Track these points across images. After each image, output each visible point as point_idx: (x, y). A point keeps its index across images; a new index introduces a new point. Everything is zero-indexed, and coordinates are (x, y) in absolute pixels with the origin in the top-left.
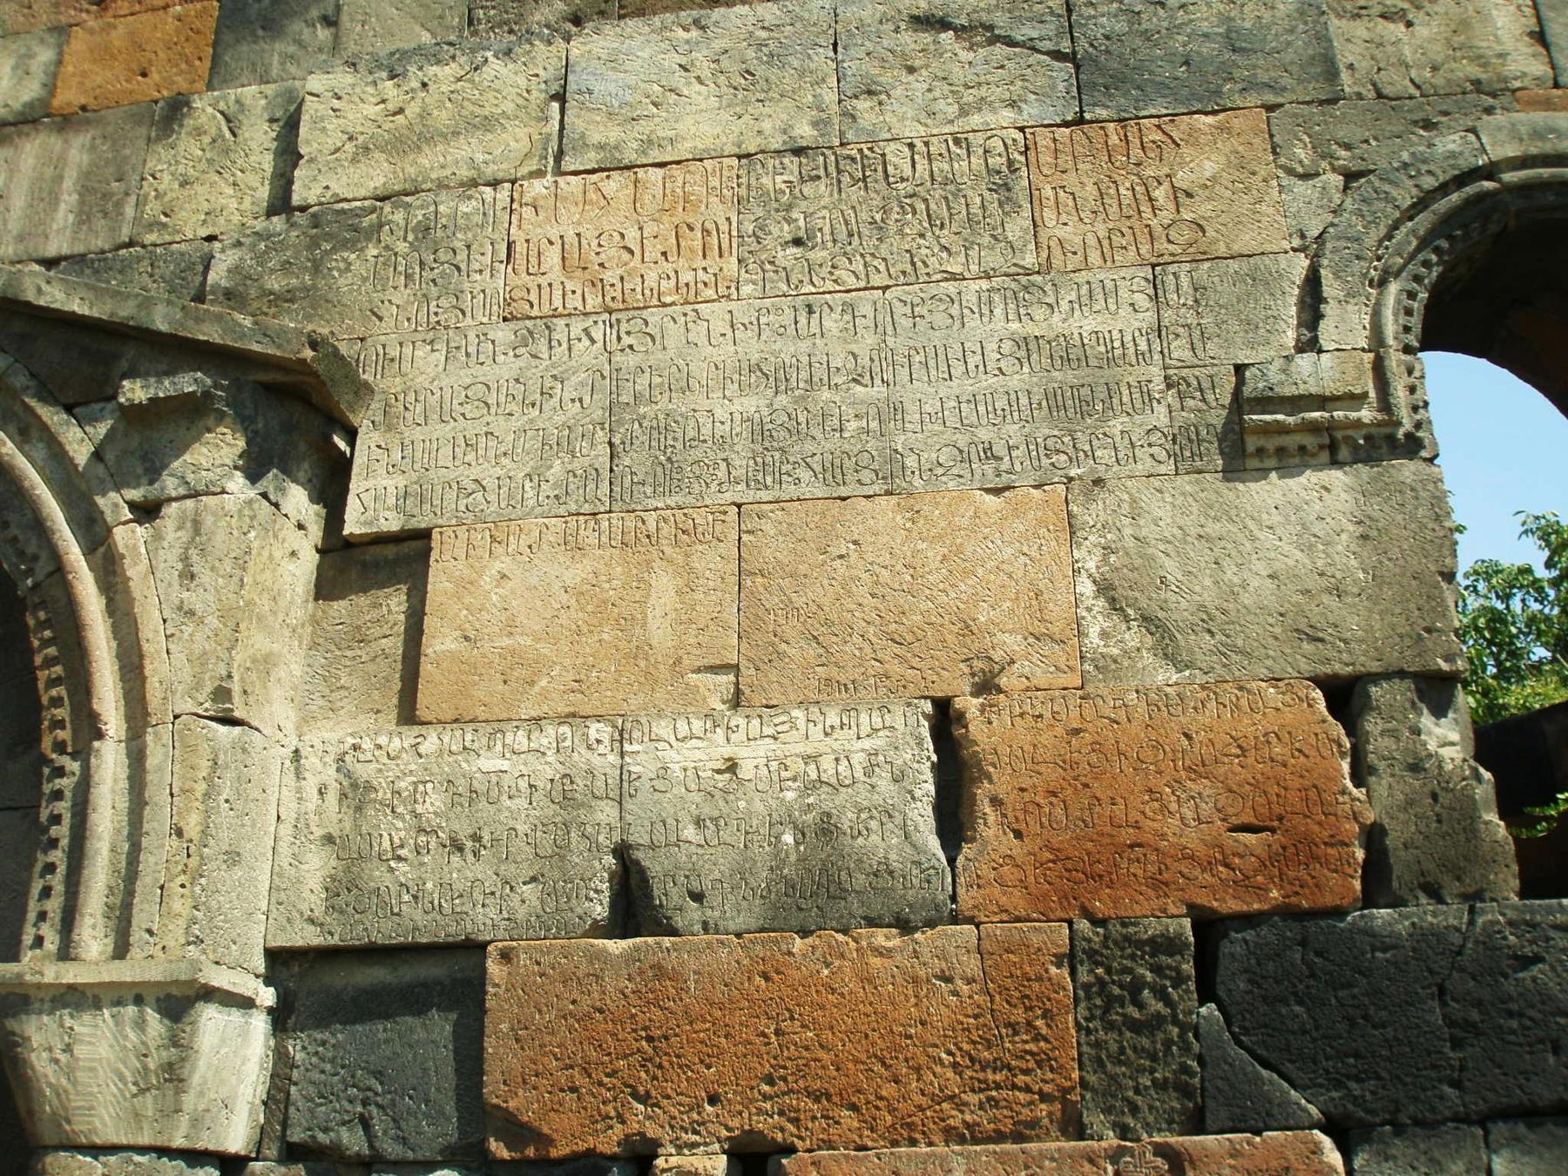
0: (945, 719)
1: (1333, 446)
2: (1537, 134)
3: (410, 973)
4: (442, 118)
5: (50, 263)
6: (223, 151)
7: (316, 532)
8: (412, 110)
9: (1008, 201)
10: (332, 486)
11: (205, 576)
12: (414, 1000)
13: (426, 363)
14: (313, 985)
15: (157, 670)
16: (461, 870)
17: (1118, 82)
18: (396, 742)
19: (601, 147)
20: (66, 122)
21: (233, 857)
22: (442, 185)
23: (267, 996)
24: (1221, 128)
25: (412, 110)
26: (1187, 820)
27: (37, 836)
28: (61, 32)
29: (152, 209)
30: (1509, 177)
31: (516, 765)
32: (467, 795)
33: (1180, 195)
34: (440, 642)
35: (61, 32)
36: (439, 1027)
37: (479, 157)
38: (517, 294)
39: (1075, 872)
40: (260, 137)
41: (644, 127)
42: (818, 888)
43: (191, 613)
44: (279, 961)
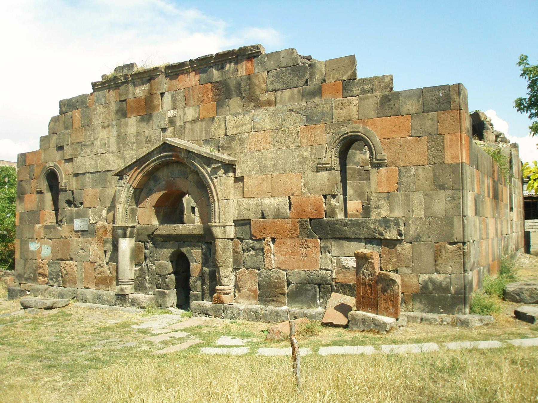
0: (289, 198)
1: (326, 169)
2: (353, 128)
3: (245, 222)
4: (241, 123)
5: (203, 140)
6: (219, 125)
7: (233, 176)
9: (298, 137)
10: (234, 171)
12: (246, 224)
13: (241, 156)
14: (238, 223)
16: (248, 213)
17: (310, 119)
20: (202, 120)
21: (228, 212)
23: (233, 224)
24: (320, 126)
26: (309, 209)
27: (211, 210)
28: (199, 105)
29: (213, 133)
30: (349, 134)
31: (253, 202)
32: (249, 205)
33: (315, 136)
34: (245, 189)
35: (199, 105)
36: (248, 227)
39: (299, 214)
40: (223, 123)
41: (262, 125)
42: (278, 215)
44: (234, 221)
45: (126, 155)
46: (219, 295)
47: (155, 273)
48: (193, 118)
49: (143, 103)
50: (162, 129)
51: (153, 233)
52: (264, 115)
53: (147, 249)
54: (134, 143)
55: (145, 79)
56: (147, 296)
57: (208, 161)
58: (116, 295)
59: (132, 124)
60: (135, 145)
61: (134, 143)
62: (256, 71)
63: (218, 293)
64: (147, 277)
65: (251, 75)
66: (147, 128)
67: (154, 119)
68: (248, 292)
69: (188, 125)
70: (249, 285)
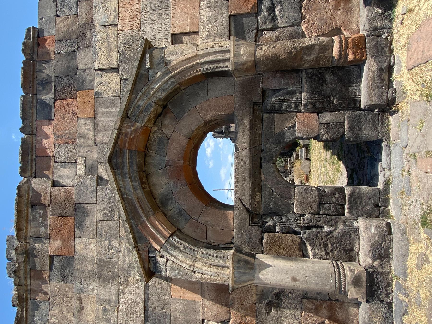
8: (103, 50)
11: (177, 51)
15: (190, 55)
16: (219, 20)
18: (202, 32)
19: (114, 18)
20: (96, 113)
22: (117, 43)
25: (103, 50)
32: (209, 21)
34: (188, 29)
37: (113, 37)
38: (137, 27)
43: (182, 52)
45: (125, 261)
46: (350, 45)
47: (316, 216)
48: (92, 129)
49: (60, 221)
50: (98, 185)
51: (247, 209)
52: (101, 10)
53: (275, 226)
54: (110, 244)
55: (29, 215)
56: (361, 229)
57: (141, 78)
58: (367, 301)
59: (87, 247)
60: (112, 242)
61: (110, 244)
62: (53, 32)
63: (346, 47)
64: (326, 229)
65: (57, 38)
66: (93, 216)
67: (83, 199)
68: (339, 13)
69: (99, 138)
70: (329, 12)
